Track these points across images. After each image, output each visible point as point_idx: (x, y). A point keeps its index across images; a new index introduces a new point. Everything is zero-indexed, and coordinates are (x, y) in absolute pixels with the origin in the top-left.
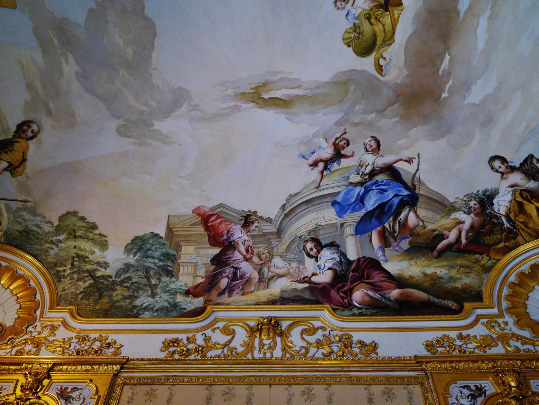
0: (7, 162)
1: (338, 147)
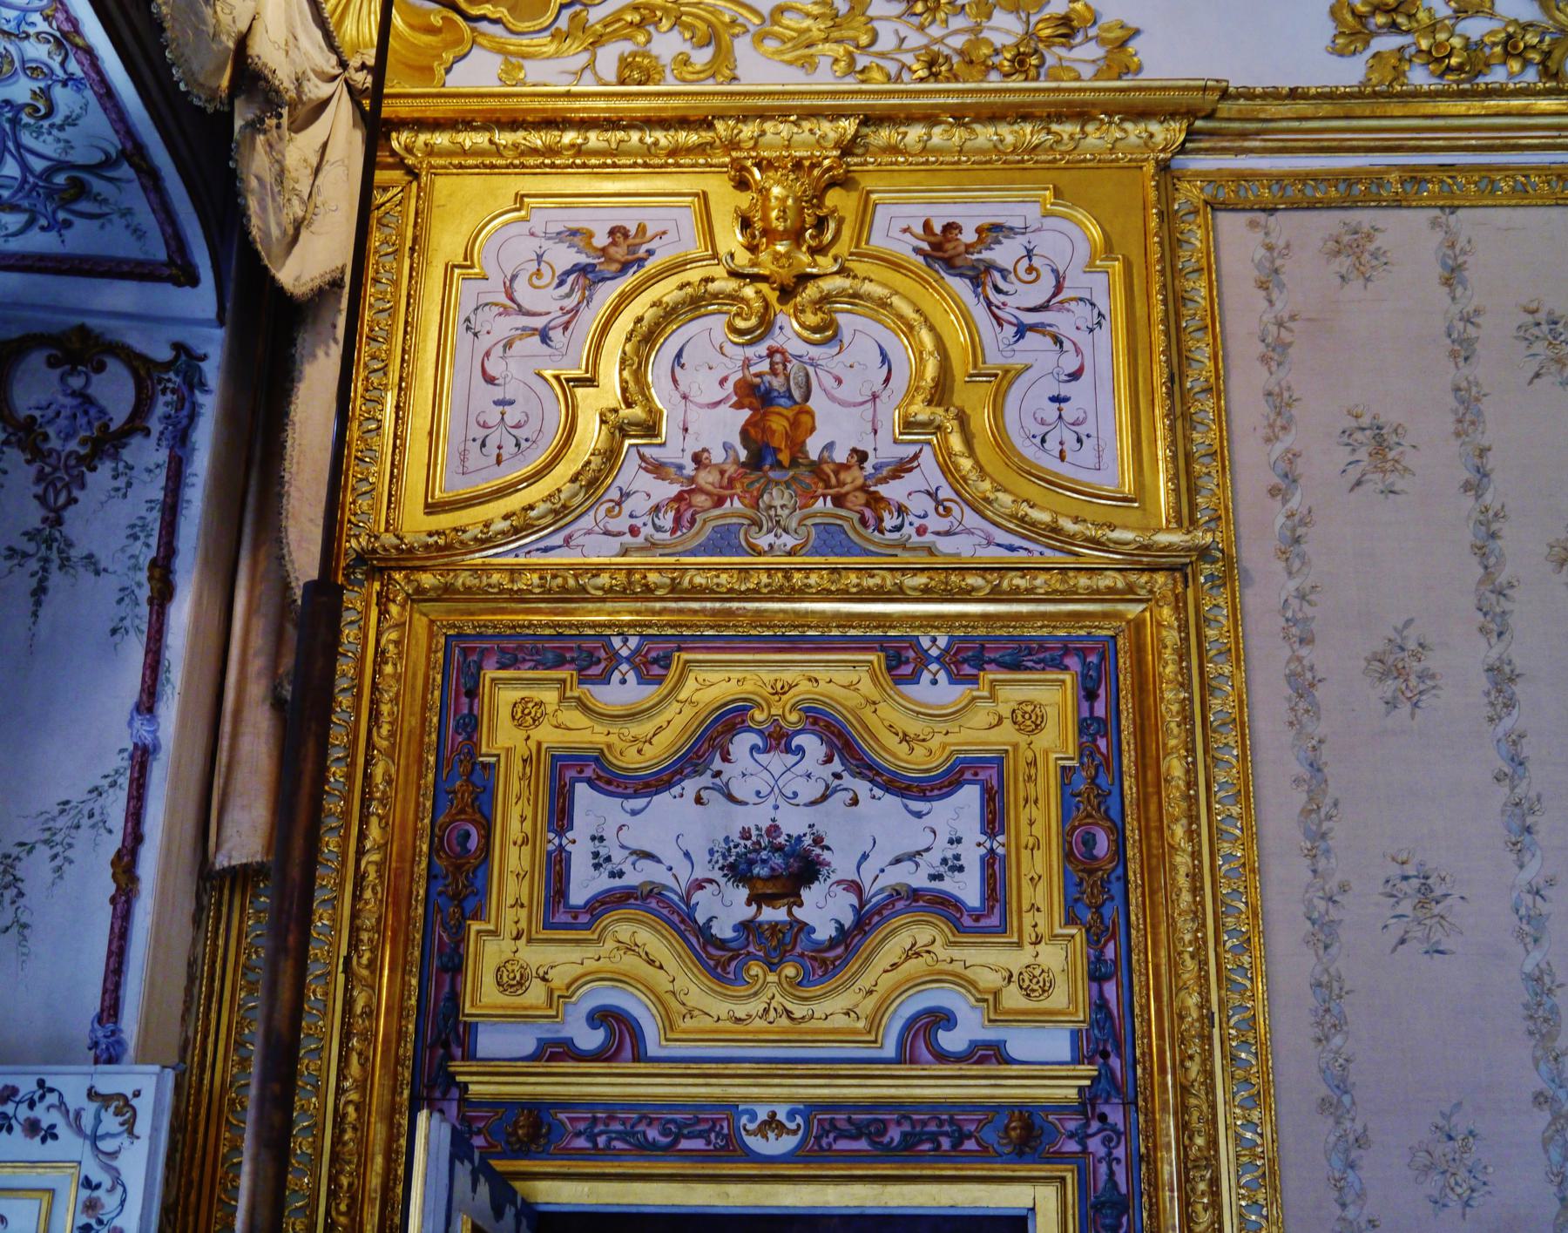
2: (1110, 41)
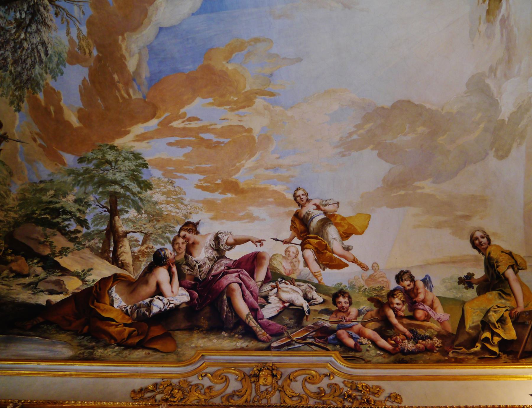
0: (508, 268)
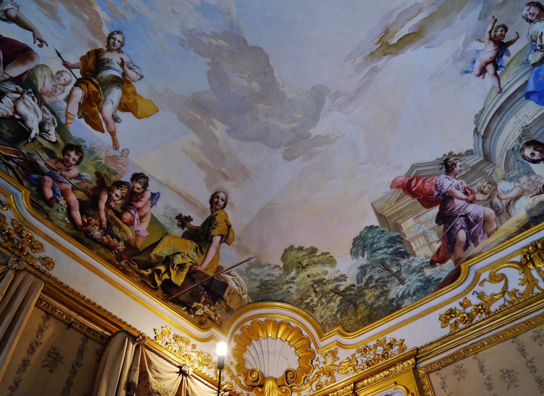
0: (219, 235)
1: (496, 39)
2: (399, 344)
